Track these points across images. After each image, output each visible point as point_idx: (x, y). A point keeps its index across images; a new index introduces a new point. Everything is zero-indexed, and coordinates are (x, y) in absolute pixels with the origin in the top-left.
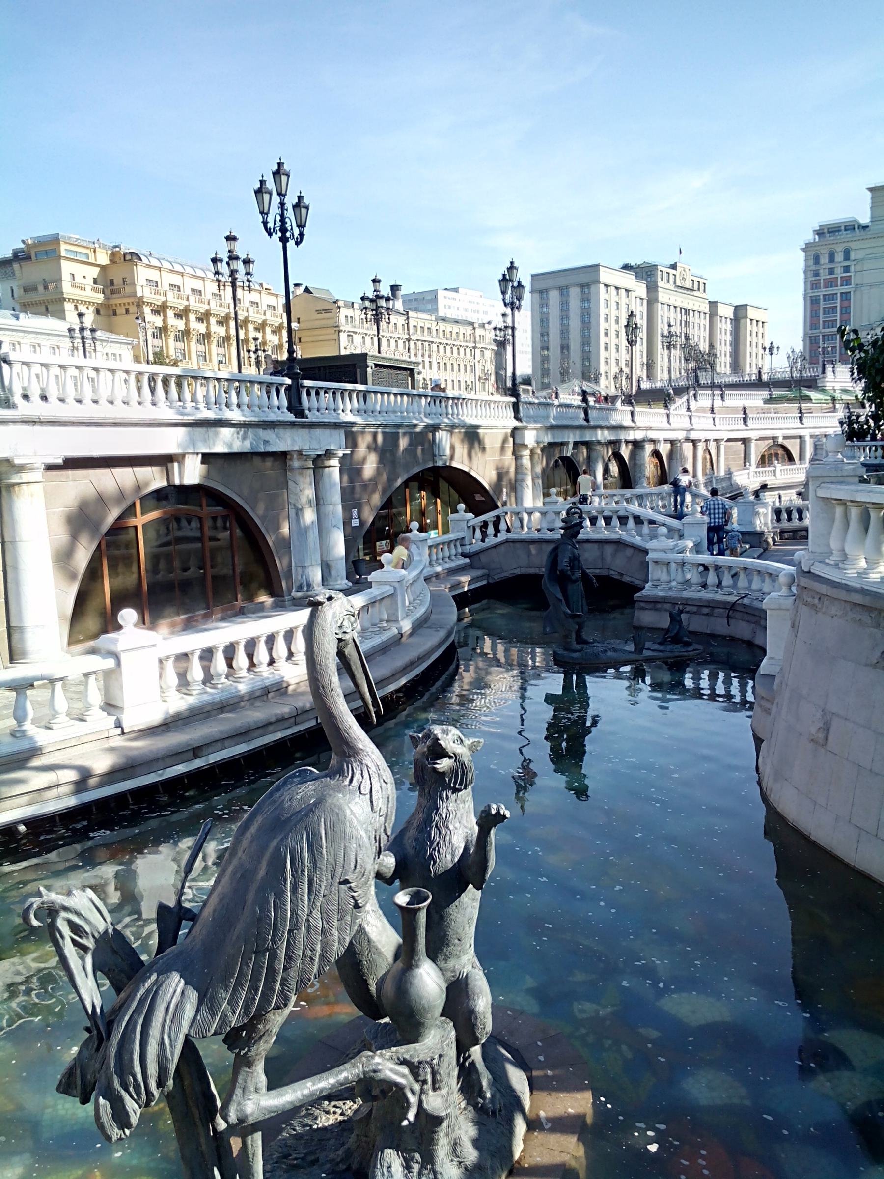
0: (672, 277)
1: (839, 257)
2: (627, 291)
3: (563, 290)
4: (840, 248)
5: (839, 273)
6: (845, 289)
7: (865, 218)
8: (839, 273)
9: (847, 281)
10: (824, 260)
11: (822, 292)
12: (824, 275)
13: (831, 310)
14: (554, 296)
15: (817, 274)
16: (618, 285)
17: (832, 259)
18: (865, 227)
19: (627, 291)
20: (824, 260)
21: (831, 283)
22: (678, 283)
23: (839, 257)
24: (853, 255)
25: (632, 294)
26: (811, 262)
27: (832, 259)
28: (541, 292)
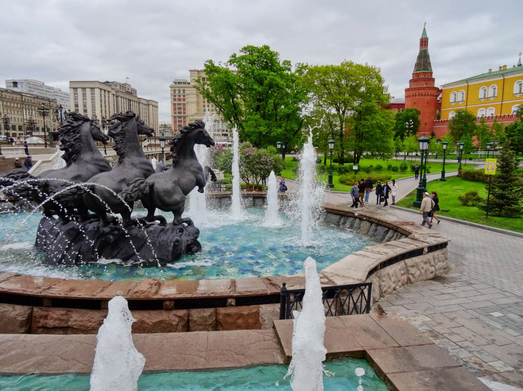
1: (182, 92)
2: (109, 92)
3: (84, 89)
4: (182, 89)
5: (182, 97)
7: (189, 81)
8: (182, 97)
9: (184, 100)
10: (177, 92)
11: (177, 102)
12: (177, 97)
13: (180, 109)
14: (80, 91)
15: (175, 96)
17: (179, 92)
18: (189, 84)
19: (109, 92)
20: (177, 92)
21: (179, 100)
22: (127, 90)
23: (182, 92)
24: (186, 92)
25: (110, 93)
26: (173, 92)
27: (179, 92)
28: (74, 88)
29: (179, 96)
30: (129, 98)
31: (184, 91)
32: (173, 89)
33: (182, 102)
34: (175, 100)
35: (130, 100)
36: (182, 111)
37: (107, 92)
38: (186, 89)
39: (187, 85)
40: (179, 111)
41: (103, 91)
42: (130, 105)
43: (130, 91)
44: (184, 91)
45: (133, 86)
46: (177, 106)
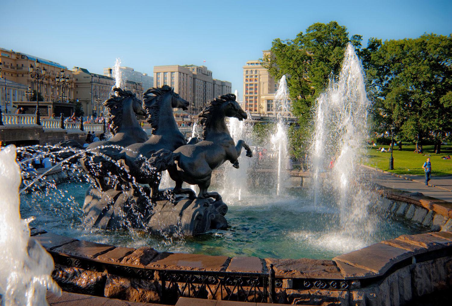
1: (254, 72)
6: (256, 82)
11: (249, 83)
19: (187, 74)
23: (254, 72)
25: (188, 76)
29: (252, 76)
31: (256, 71)
32: (246, 70)
33: (254, 82)
34: (247, 80)
36: (254, 91)
37: (185, 75)
40: (251, 91)
41: (182, 74)
42: (206, 86)
43: (206, 73)
44: (256, 71)
46: (249, 87)
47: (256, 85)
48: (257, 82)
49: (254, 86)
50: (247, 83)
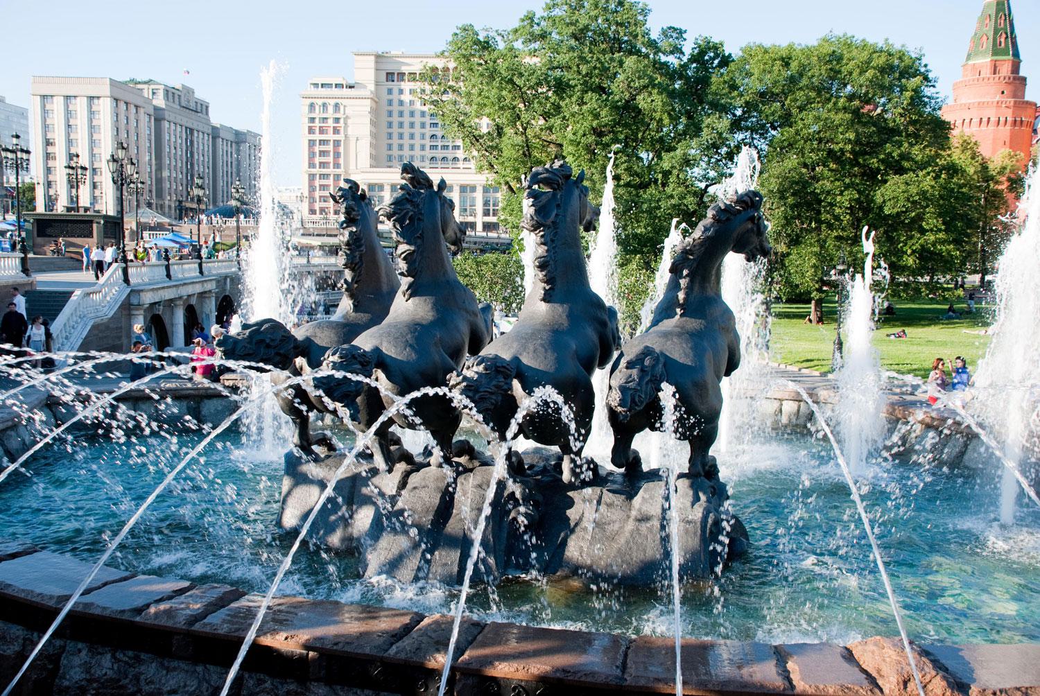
0: (176, 97)
1: (331, 109)
4: (333, 102)
6: (337, 137)
11: (317, 137)
16: (128, 101)
19: (137, 107)
22: (183, 104)
23: (331, 109)
25: (141, 111)
30: (190, 126)
31: (337, 106)
32: (308, 101)
33: (330, 136)
34: (311, 130)
35: (192, 130)
36: (330, 159)
38: (344, 102)
39: (346, 92)
40: (323, 159)
41: (123, 106)
42: (192, 142)
43: (192, 106)
44: (337, 106)
45: (200, 94)
46: (317, 149)
47: (337, 143)
48: (341, 137)
49: (330, 147)
50: (312, 137)
